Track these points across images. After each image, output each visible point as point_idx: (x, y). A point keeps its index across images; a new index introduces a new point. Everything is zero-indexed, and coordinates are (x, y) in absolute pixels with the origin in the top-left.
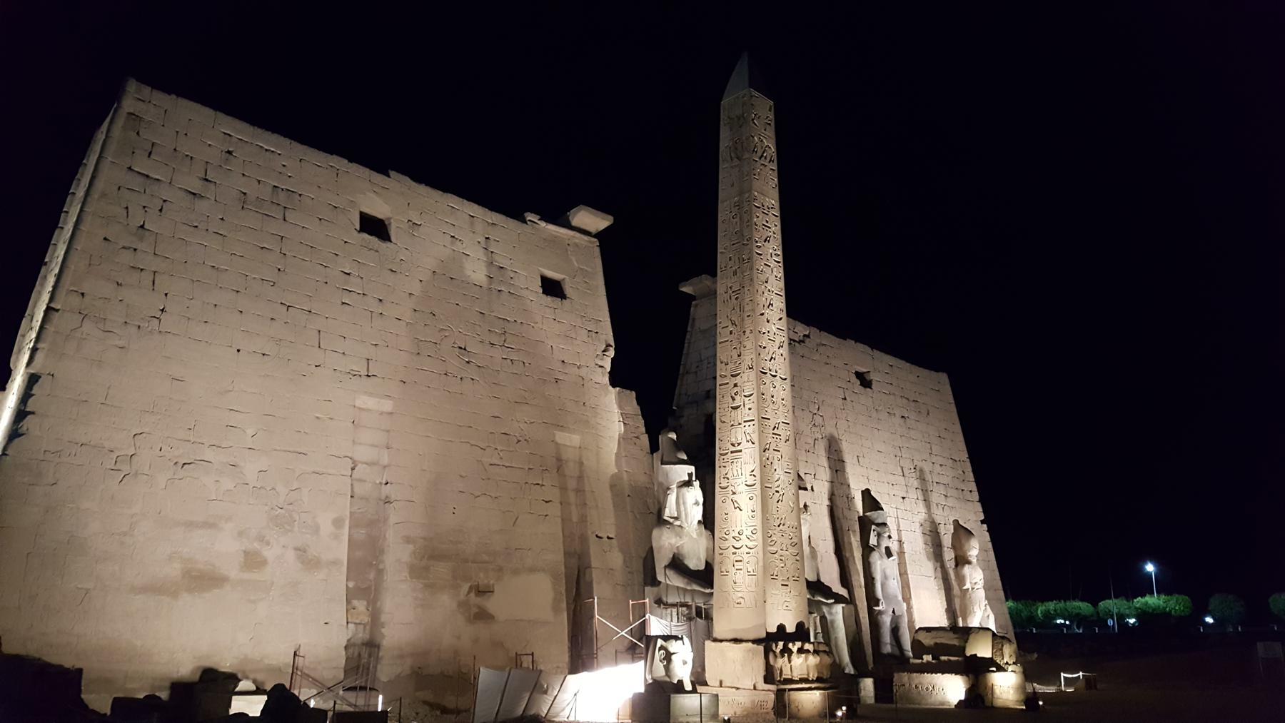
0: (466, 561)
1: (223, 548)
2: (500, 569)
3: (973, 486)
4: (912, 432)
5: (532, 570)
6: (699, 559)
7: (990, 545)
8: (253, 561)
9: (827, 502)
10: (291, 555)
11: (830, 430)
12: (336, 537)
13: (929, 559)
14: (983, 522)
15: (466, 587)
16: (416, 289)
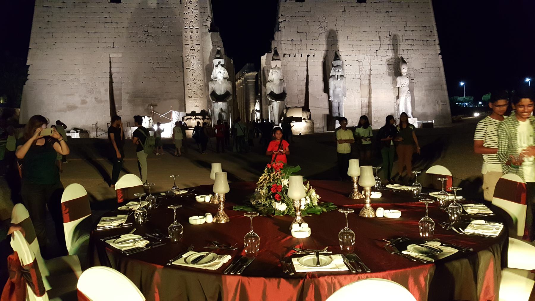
0: (147, 97)
1: (76, 100)
2: (159, 99)
3: (436, 38)
4: (392, 18)
5: (171, 99)
6: (221, 91)
7: (442, 65)
8: (84, 102)
9: (322, 60)
10: (94, 100)
11: (331, 26)
12: (106, 94)
13: (389, 75)
14: (439, 54)
15: (147, 105)
16: (129, 15)
